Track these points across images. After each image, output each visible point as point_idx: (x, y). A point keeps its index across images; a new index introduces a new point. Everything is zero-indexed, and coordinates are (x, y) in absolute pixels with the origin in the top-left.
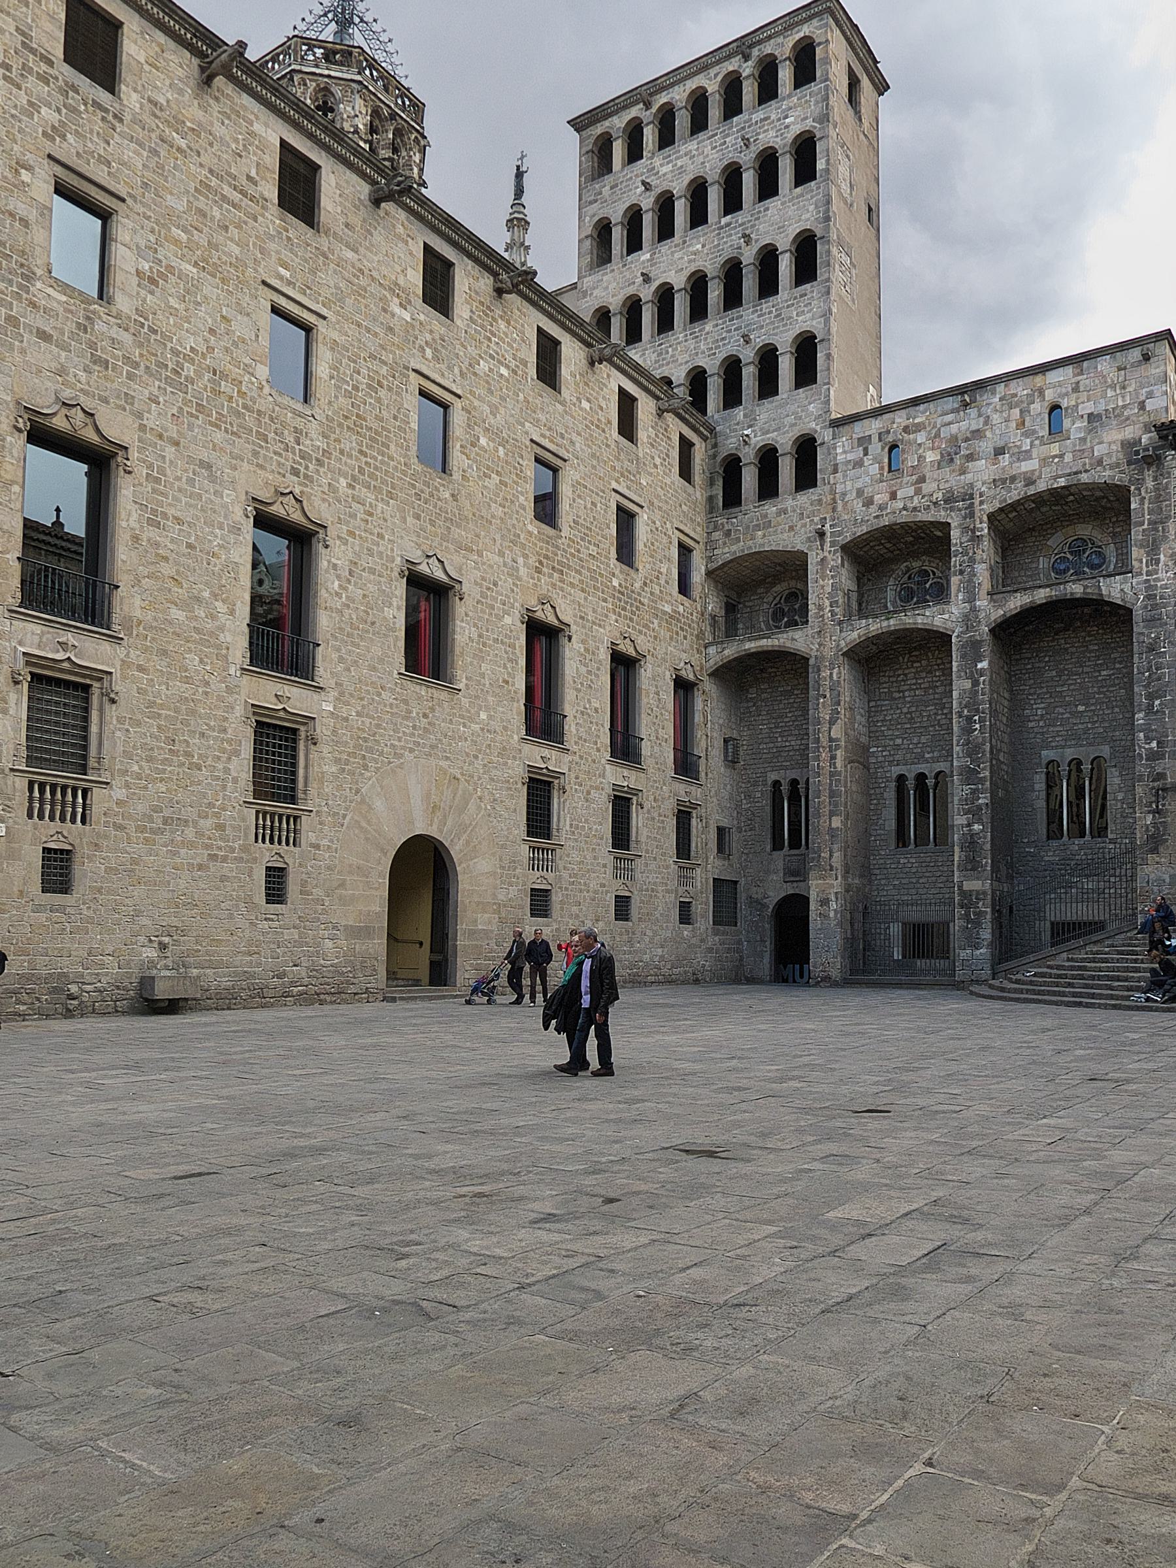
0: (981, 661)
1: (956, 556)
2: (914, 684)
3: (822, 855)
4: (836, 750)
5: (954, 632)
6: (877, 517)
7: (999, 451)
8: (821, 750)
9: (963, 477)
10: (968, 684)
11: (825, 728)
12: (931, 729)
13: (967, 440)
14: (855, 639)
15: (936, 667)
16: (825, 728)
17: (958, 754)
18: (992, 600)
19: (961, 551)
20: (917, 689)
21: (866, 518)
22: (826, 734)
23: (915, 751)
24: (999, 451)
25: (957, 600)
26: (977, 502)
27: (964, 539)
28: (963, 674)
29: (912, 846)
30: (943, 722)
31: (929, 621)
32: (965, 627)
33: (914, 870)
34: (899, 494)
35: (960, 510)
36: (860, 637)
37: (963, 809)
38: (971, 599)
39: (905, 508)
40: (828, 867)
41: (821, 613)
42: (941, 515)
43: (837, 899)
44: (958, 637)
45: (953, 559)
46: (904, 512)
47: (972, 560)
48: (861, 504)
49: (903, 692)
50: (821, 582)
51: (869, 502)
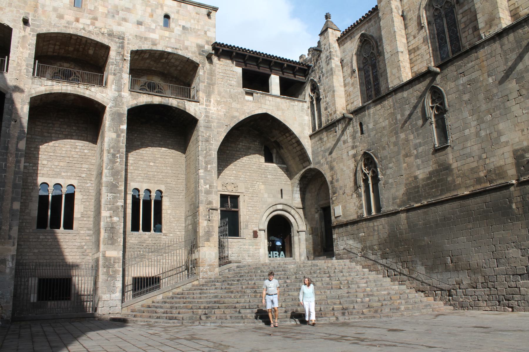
0: (123, 125)
1: (112, 65)
2: (59, 131)
3: (3, 227)
4: (21, 157)
5: (108, 104)
6: (66, 27)
7: (140, 23)
8: (9, 155)
9: (119, 27)
10: (114, 135)
11: (14, 141)
12: (67, 159)
13: (122, 10)
14: (42, 91)
15: (74, 124)
16: (14, 141)
17: (106, 174)
18: (130, 93)
19: (115, 63)
20: (60, 134)
21: (58, 25)
22: (14, 146)
23: (56, 170)
24: (140, 23)
25: (111, 88)
26: (126, 42)
27: (118, 58)
28: (112, 129)
29: (48, 228)
30: (75, 156)
31: (93, 94)
32: (114, 105)
33: (49, 244)
34: (81, 20)
35: (116, 43)
36: (46, 90)
37: (107, 207)
38: (119, 90)
39: (84, 29)
40: (7, 237)
41: (19, 68)
42: (105, 41)
43: (13, 259)
44: (110, 108)
45: (111, 66)
46: (83, 31)
47: (121, 71)
48: (55, 16)
49: (51, 133)
50: (21, 50)
51: (61, 17)
